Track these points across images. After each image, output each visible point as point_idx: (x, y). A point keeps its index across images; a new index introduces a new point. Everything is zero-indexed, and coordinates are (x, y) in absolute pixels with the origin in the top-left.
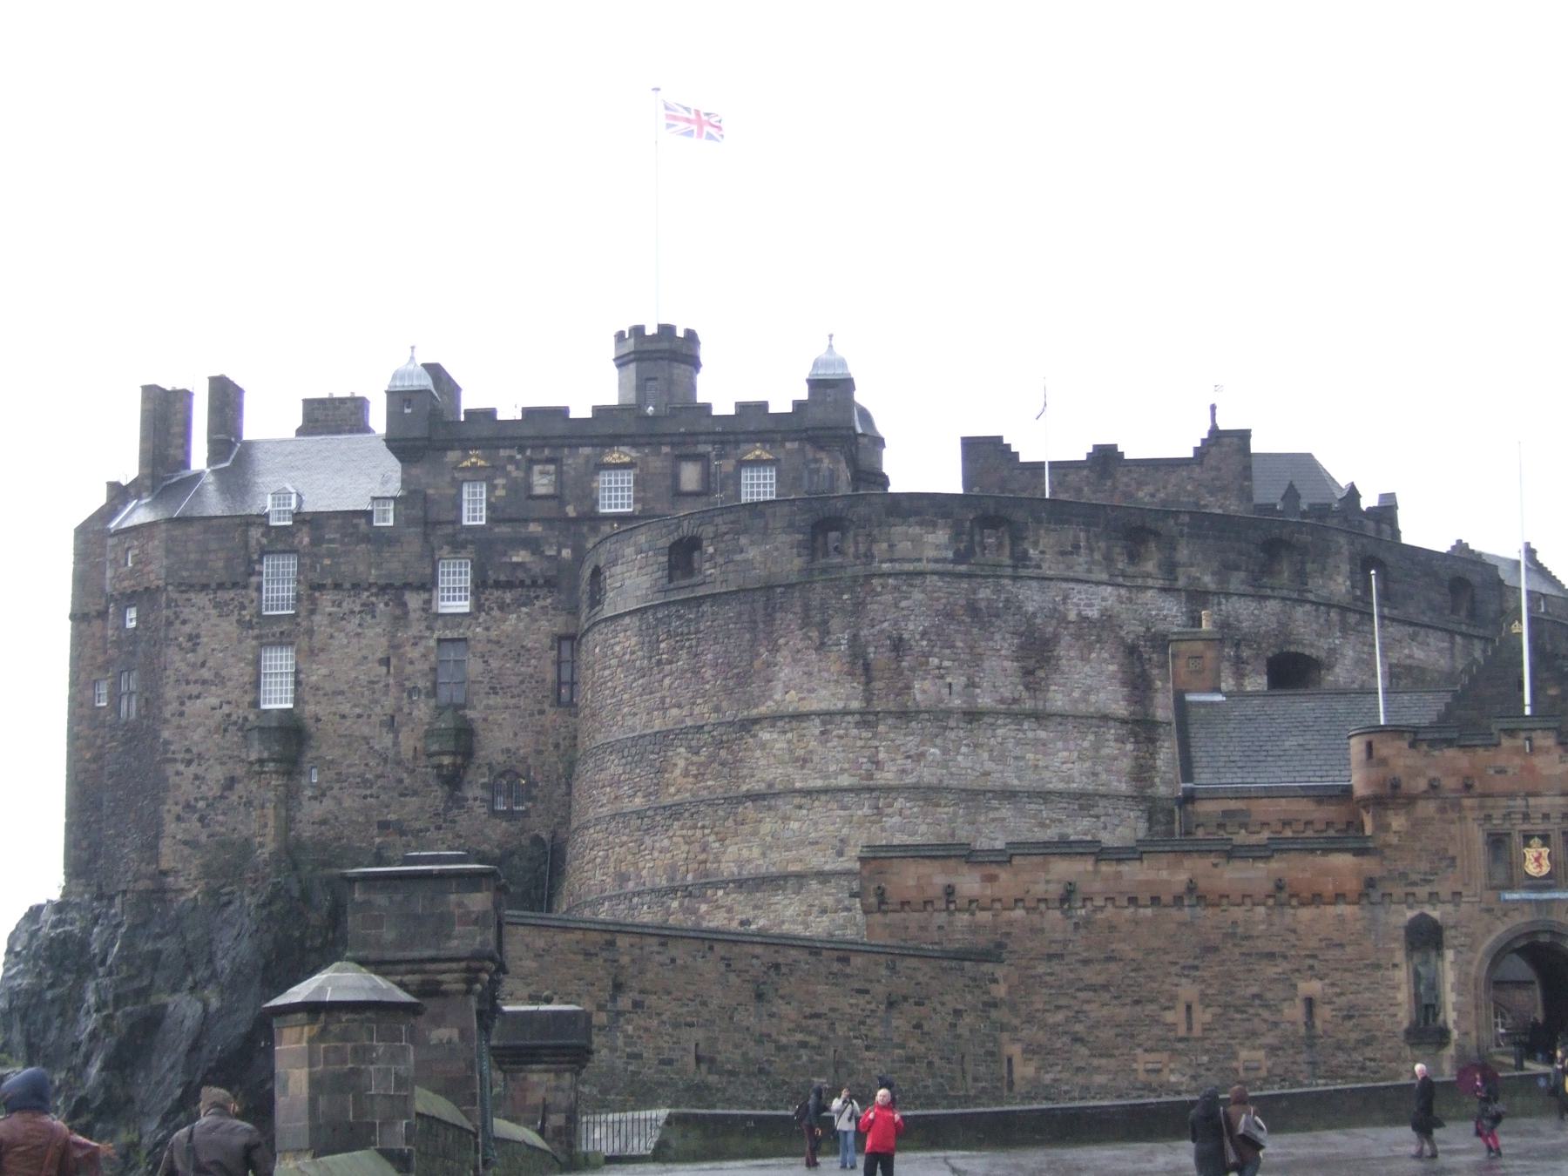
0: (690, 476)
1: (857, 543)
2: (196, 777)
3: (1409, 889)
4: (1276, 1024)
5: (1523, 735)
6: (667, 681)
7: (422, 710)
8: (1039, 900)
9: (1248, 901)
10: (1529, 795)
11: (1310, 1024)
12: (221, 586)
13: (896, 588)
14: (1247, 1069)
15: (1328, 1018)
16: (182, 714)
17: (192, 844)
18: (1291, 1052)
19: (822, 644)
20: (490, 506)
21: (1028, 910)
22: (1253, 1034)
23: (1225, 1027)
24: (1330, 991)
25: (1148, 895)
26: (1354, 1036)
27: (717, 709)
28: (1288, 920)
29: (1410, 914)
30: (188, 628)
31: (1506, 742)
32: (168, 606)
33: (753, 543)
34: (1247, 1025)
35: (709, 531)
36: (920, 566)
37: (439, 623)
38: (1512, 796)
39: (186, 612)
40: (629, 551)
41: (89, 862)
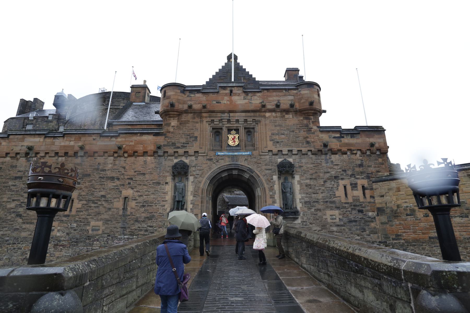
3: (176, 150)
4: (110, 209)
5: (229, 89)
8: (17, 154)
9: (106, 155)
10: (230, 112)
11: (124, 209)
14: (93, 230)
15: (134, 207)
18: (114, 222)
21: (11, 157)
22: (99, 213)
23: (87, 210)
24: (136, 194)
25: (63, 151)
26: (144, 215)
28: (122, 163)
29: (176, 161)
31: (222, 91)
34: (97, 210)
36: (119, 107)
38: (223, 112)
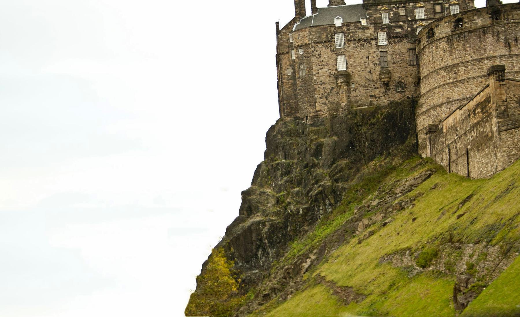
0: (438, 8)
1: (504, 16)
2: (324, 88)
6: (457, 52)
7: (378, 69)
12: (325, 42)
13: (515, 26)
16: (318, 73)
17: (324, 104)
19: (498, 40)
20: (389, 19)
27: (471, 57)
30: (318, 53)
32: (312, 48)
33: (478, 18)
35: (466, 16)
37: (380, 48)
39: (317, 49)
40: (442, 23)
41: (290, 112)
